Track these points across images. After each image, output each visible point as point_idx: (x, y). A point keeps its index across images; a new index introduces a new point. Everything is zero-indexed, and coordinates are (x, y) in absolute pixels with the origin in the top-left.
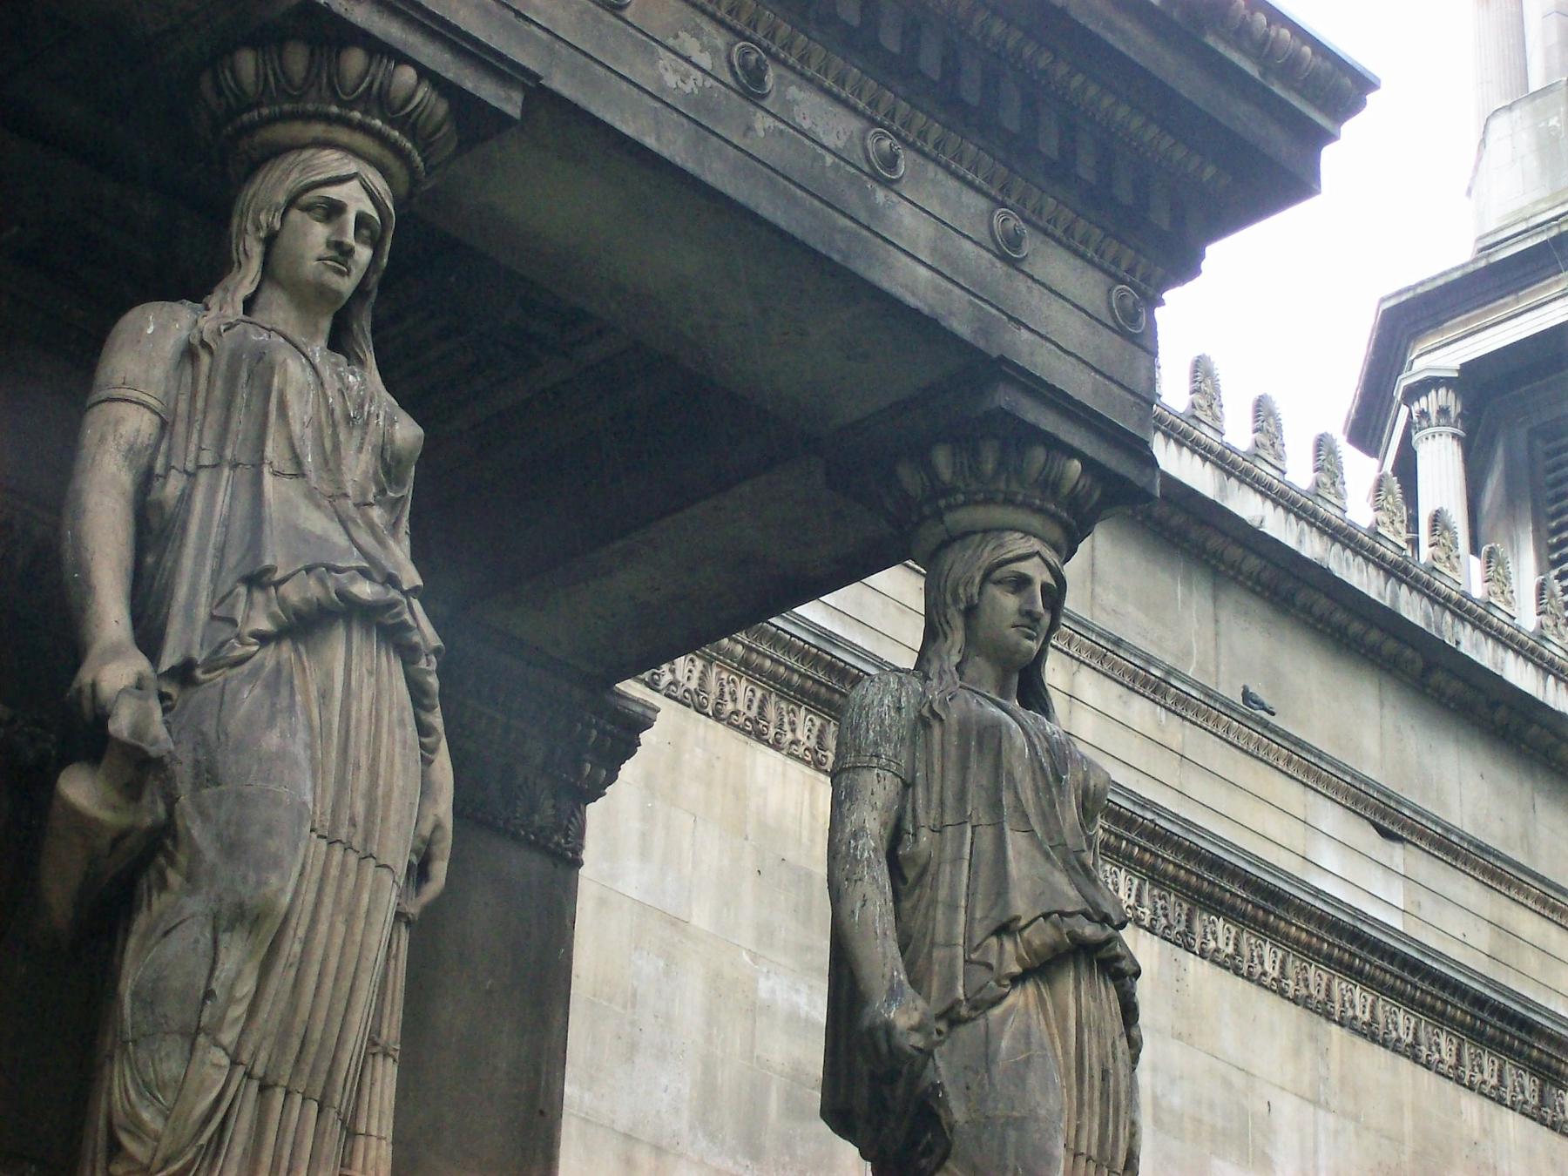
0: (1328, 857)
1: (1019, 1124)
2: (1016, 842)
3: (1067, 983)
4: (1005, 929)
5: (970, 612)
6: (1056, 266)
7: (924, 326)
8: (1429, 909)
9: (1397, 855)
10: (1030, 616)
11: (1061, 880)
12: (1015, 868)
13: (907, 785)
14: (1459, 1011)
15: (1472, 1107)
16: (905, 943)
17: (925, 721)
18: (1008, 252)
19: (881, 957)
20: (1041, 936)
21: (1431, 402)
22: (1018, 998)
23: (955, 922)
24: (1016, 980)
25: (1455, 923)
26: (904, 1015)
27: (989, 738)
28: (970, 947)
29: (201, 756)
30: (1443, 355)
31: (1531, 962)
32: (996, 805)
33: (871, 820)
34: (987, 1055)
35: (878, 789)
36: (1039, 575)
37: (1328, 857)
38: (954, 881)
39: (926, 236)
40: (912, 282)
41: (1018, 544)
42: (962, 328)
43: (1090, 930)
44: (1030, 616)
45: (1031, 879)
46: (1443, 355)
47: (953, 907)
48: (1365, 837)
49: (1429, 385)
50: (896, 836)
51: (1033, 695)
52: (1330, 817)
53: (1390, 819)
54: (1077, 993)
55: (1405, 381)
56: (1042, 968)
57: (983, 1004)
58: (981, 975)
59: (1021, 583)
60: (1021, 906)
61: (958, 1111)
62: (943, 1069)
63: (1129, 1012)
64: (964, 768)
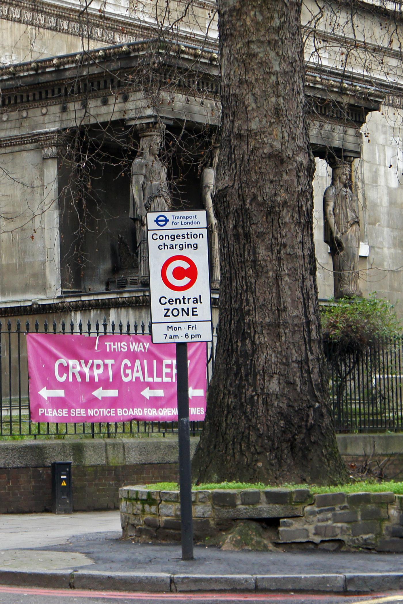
1: (352, 247)
2: (348, 210)
4: (348, 222)
13: (335, 203)
20: (351, 222)
23: (342, 222)
29: (240, 192)
32: (346, 206)
34: (347, 239)
38: (342, 216)
43: (356, 220)
47: (342, 220)
54: (355, 227)
57: (346, 232)
58: (346, 228)
61: (344, 245)
62: (343, 241)
64: (342, 201)
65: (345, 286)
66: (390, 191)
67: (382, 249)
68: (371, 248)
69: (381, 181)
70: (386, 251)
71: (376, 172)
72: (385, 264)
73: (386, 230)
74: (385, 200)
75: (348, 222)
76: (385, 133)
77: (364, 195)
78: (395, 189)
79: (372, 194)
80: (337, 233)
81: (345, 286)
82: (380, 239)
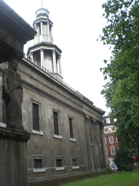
0: (27, 80)
2: (15, 80)
3: (18, 89)
4: (15, 86)
5: (12, 65)
6: (18, 43)
7: (9, 46)
8: (33, 83)
9: (31, 79)
10: (16, 65)
11: (18, 83)
12: (15, 82)
13: (8, 76)
14: (35, 88)
15: (35, 94)
16: (8, 87)
17: (9, 72)
18: (15, 41)
19: (6, 87)
20: (17, 86)
21: (31, 53)
22: (16, 91)
24: (15, 89)
25: (34, 83)
26: (8, 92)
27: (13, 73)
28: (12, 87)
30: (32, 51)
31: (38, 85)
32: (14, 78)
33: (5, 79)
35: (6, 76)
36: (16, 62)
37: (27, 80)
39: (9, 41)
40: (9, 43)
41: (15, 61)
42: (12, 46)
43: (20, 86)
44: (16, 65)
45: (16, 83)
46: (32, 51)
48: (29, 78)
50: (7, 80)
51: (16, 71)
52: (28, 77)
53: (31, 77)
54: (19, 90)
55: (30, 52)
56: (17, 88)
59: (15, 63)
60: (15, 84)
61: (12, 98)
62: (11, 95)
63: (22, 91)
65: (11, 121)
66: (49, 119)
67: (47, 134)
68: (44, 133)
69: (47, 117)
70: (48, 134)
71: (45, 114)
72: (48, 137)
73: (48, 129)
74: (47, 121)
75: (15, 86)
76: (47, 105)
77: (42, 119)
78: (50, 119)
79: (44, 119)
80: (7, 91)
81: (11, 121)
82: (46, 131)
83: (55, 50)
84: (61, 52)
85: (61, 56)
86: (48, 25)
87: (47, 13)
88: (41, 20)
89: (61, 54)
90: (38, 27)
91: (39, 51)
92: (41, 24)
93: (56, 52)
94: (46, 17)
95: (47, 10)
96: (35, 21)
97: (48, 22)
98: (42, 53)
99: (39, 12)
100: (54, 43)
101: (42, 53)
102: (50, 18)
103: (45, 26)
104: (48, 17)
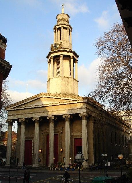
30: (52, 55)
46: (52, 55)
49: (52, 57)
83: (73, 57)
84: (78, 57)
85: (77, 61)
86: (68, 30)
87: (68, 19)
88: (63, 25)
89: (78, 59)
90: (59, 31)
91: (59, 56)
92: (62, 29)
93: (74, 57)
94: (65, 23)
95: (68, 15)
96: (56, 26)
97: (68, 28)
98: (61, 58)
99: (60, 17)
100: (73, 50)
101: (61, 58)
102: (70, 24)
103: (65, 30)
104: (68, 22)
